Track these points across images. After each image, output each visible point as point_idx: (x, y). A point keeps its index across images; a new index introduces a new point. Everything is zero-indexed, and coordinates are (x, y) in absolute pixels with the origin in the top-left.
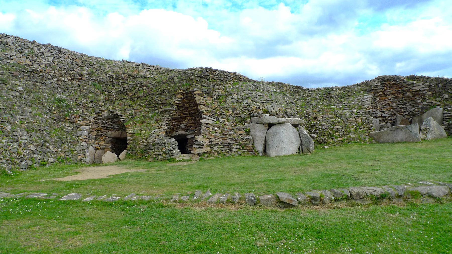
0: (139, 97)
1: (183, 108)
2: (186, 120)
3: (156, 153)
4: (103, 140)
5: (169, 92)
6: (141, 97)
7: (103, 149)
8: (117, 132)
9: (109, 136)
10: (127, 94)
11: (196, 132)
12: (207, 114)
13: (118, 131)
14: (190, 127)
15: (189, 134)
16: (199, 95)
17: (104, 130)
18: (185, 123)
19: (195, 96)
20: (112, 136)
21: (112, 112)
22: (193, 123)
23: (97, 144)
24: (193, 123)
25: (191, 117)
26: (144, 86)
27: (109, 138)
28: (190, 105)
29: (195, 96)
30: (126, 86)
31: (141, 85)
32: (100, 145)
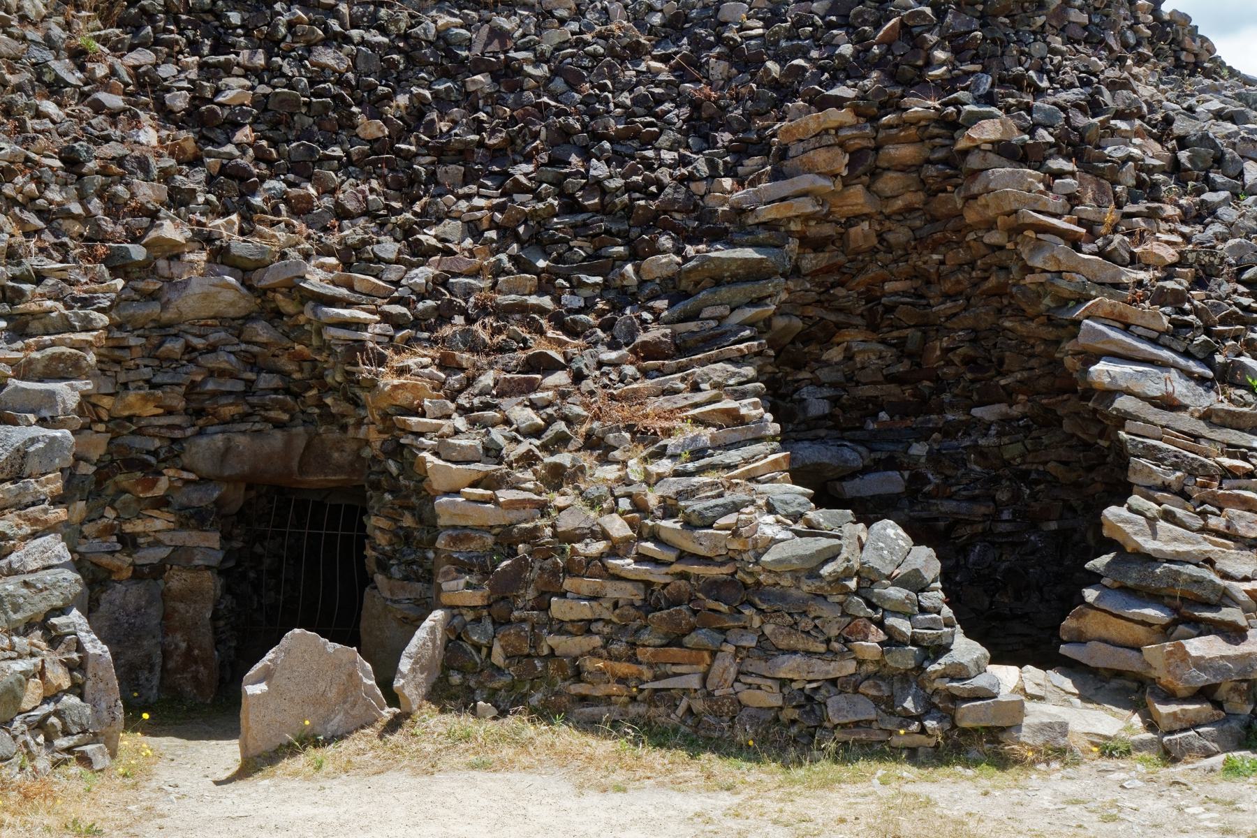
0: (442, 153)
1: (823, 259)
2: (835, 354)
3: (787, 667)
4: (161, 503)
5: (701, 125)
6: (463, 154)
7: (158, 571)
8: (277, 439)
9: (206, 467)
10: (348, 123)
11: (919, 449)
12: (1132, 313)
13: (279, 425)
14: (872, 407)
15: (865, 470)
16: (1006, 151)
17: (170, 412)
18: (824, 374)
19: (974, 161)
20: (234, 468)
21: (245, 269)
22: (890, 379)
23: (108, 530)
24: (890, 379)
25: (873, 327)
26: (478, 66)
27: (204, 480)
28: (880, 236)
29: (974, 161)
30: (327, 57)
31: (454, 57)
32: (129, 542)
